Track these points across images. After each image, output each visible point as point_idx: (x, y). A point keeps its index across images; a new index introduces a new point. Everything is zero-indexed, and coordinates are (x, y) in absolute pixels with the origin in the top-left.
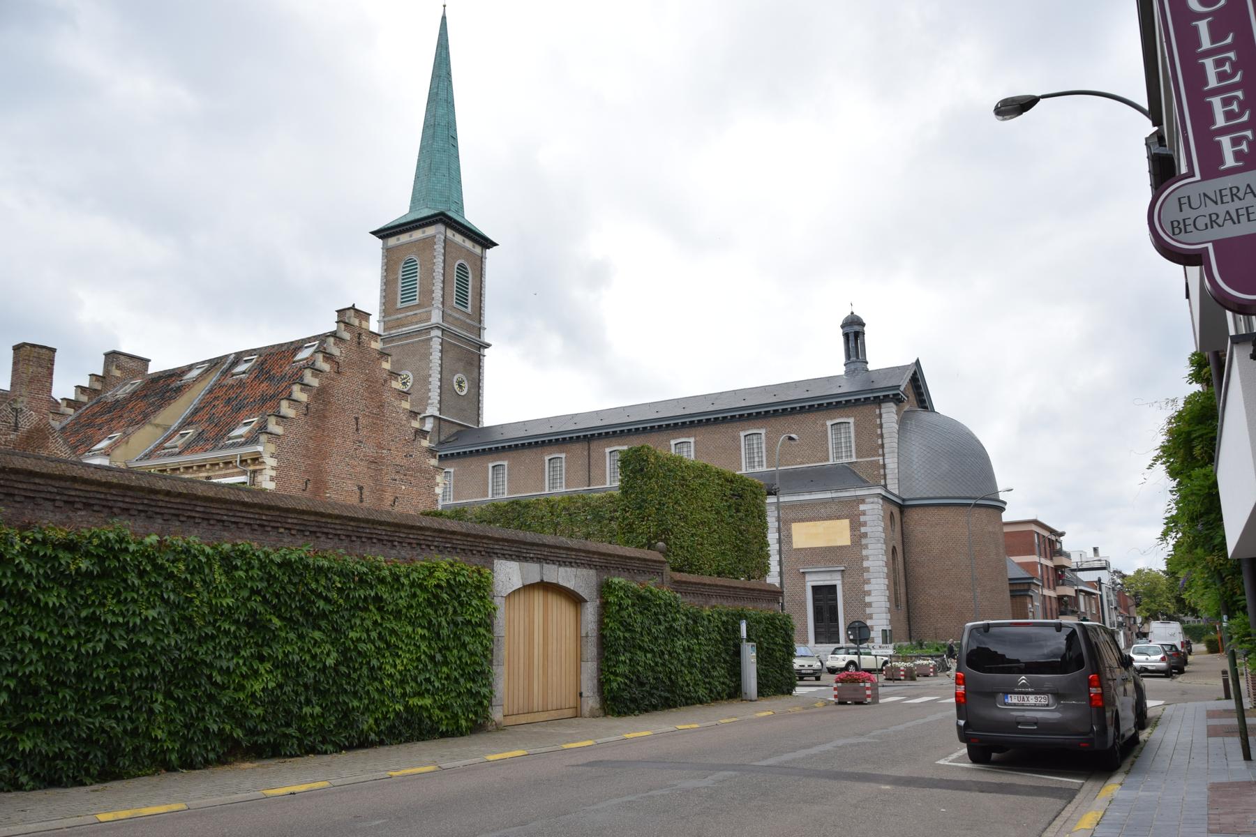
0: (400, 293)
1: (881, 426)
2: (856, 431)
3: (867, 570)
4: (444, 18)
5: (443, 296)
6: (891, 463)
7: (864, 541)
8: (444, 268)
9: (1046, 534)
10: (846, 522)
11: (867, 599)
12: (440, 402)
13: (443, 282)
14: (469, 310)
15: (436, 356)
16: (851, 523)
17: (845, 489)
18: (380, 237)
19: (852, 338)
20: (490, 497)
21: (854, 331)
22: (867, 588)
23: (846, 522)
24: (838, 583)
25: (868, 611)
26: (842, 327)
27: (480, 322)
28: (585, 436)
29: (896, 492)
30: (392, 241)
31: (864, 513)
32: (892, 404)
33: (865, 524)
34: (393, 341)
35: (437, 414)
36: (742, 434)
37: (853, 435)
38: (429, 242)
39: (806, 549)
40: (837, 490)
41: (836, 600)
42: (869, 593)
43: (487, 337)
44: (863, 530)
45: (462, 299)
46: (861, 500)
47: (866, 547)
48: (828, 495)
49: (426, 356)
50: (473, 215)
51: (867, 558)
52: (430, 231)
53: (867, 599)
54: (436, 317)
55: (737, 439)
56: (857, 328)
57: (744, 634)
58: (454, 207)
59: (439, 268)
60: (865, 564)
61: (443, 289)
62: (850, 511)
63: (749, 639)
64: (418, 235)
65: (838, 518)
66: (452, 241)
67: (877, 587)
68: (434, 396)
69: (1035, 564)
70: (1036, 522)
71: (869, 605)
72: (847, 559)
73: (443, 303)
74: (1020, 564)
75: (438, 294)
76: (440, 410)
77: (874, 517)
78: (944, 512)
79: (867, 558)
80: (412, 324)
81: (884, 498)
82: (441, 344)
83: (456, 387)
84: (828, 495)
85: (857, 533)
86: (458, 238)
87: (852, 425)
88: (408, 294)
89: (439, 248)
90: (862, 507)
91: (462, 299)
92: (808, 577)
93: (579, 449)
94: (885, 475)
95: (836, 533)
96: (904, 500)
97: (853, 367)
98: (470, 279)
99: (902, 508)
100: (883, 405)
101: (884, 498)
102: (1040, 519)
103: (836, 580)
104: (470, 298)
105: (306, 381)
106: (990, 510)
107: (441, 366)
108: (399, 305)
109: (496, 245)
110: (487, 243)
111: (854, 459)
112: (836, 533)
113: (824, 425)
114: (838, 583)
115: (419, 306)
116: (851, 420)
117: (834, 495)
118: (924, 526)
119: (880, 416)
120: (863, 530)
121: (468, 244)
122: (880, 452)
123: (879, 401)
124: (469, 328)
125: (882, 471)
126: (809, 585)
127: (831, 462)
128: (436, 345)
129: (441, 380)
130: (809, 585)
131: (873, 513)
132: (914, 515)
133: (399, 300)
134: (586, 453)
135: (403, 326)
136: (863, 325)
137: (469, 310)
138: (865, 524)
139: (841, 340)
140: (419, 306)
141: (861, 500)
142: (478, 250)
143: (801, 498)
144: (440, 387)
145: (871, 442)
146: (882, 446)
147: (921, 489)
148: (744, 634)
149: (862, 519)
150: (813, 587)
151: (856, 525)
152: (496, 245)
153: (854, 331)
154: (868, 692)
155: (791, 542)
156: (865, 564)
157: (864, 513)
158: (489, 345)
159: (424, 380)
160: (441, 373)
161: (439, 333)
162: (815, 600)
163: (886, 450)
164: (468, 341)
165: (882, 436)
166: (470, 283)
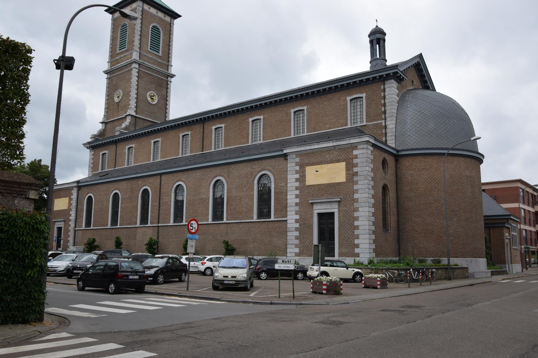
0: (118, 44)
1: (384, 98)
2: (367, 103)
3: (357, 200)
5: (140, 44)
6: (391, 124)
7: (355, 179)
8: (141, 27)
9: (531, 191)
10: (343, 164)
11: (356, 223)
12: (136, 107)
13: (141, 35)
14: (160, 54)
15: (134, 80)
16: (347, 165)
17: (342, 139)
18: (111, 13)
19: (375, 42)
20: (151, 161)
21: (377, 38)
22: (356, 214)
23: (343, 164)
24: (336, 211)
25: (356, 232)
27: (168, 61)
28: (201, 119)
29: (393, 146)
31: (356, 157)
32: (393, 81)
33: (356, 165)
34: (114, 73)
35: (134, 114)
36: (292, 111)
37: (364, 106)
39: (314, 185)
40: (337, 140)
41: (333, 223)
42: (357, 219)
43: (173, 70)
44: (355, 170)
45: (155, 46)
46: (354, 147)
47: (357, 183)
48: (331, 144)
49: (129, 80)
51: (357, 191)
53: (356, 223)
54: (135, 56)
55: (289, 114)
56: (379, 36)
60: (356, 196)
61: (140, 40)
62: (346, 156)
65: (338, 161)
66: (148, 12)
68: (133, 103)
69: (519, 209)
70: (520, 181)
71: (357, 228)
72: (341, 192)
73: (140, 48)
74: (507, 209)
76: (136, 112)
77: (363, 160)
78: (429, 160)
79: (357, 191)
81: (374, 145)
82: (138, 73)
83: (149, 99)
84: (331, 144)
85: (351, 172)
86: (153, 11)
87: (364, 98)
88: (122, 46)
90: (355, 152)
91: (155, 46)
92: (315, 207)
93: (198, 128)
94: (386, 134)
95: (333, 173)
96: (398, 151)
97: (375, 63)
99: (397, 157)
100: (386, 82)
101: (374, 145)
103: (334, 209)
104: (161, 47)
106: (468, 160)
107: (137, 85)
108: (118, 52)
109: (180, 16)
110: (175, 16)
111: (365, 124)
112: (333, 173)
114: (336, 211)
115: (127, 51)
116: (364, 95)
117: (335, 144)
118: (412, 170)
119: (384, 90)
120: (355, 170)
121: (160, 15)
122: (383, 116)
124: (159, 64)
125: (384, 131)
126: (316, 212)
127: (349, 126)
128: (135, 73)
129: (137, 94)
130: (316, 212)
131: (364, 156)
132: (406, 163)
133: (118, 49)
134: (202, 130)
136: (385, 34)
137: (160, 54)
138: (356, 165)
139: (368, 45)
140: (127, 51)
141: (354, 147)
142: (168, 19)
143: (312, 147)
144: (137, 98)
145: (377, 111)
146: (385, 112)
147: (413, 141)
149: (355, 161)
150: (320, 215)
151: (350, 166)
152: (180, 16)
153: (377, 38)
155: (305, 181)
156: (356, 196)
157: (356, 157)
158: (173, 76)
159: (127, 94)
160: (137, 89)
161: (137, 66)
162: (320, 224)
163: (387, 115)
164: (159, 72)
165: (384, 105)
166: (161, 38)
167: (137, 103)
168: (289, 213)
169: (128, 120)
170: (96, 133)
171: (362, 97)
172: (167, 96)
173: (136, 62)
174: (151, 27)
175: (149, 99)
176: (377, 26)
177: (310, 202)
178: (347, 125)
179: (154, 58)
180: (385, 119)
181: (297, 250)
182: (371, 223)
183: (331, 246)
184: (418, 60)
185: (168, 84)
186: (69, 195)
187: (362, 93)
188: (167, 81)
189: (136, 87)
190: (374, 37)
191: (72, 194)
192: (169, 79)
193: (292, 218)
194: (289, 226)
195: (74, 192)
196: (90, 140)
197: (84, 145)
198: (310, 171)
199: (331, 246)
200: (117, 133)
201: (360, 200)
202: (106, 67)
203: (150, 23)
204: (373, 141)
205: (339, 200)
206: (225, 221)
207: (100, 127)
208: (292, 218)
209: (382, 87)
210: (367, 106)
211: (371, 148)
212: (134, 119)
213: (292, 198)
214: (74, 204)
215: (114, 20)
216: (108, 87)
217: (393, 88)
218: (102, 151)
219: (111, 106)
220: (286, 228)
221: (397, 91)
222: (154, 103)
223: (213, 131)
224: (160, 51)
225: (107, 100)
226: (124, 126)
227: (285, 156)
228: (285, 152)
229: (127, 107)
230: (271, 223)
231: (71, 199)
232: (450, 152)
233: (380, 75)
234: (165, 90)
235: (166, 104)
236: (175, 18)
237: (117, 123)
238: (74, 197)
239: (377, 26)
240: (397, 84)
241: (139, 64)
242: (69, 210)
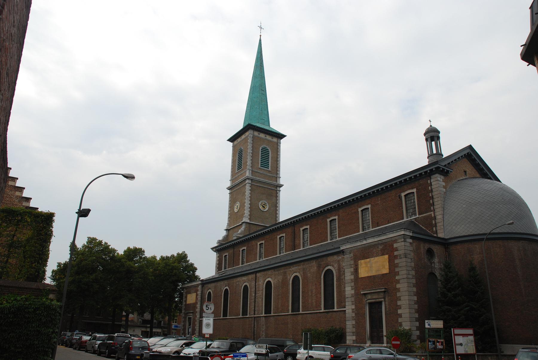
4: (260, 40)
12: (250, 215)
26: (425, 135)
30: (236, 142)
32: (437, 175)
35: (248, 221)
41: (382, 312)
43: (282, 181)
45: (265, 163)
46: (395, 240)
50: (275, 125)
56: (432, 134)
66: (258, 137)
68: (247, 212)
72: (386, 283)
76: (250, 219)
83: (261, 207)
86: (262, 135)
91: (265, 163)
93: (290, 230)
101: (412, 237)
112: (375, 266)
113: (400, 197)
121: (269, 138)
128: (248, 187)
133: (237, 169)
136: (439, 132)
137: (270, 169)
142: (275, 140)
146: (433, 204)
150: (370, 304)
158: (281, 186)
159: (242, 206)
160: (250, 201)
161: (250, 182)
167: (250, 212)
168: (347, 304)
169: (243, 227)
170: (221, 238)
171: (413, 193)
172: (277, 203)
173: (249, 179)
174: (261, 149)
175: (261, 207)
176: (431, 126)
177: (362, 293)
179: (264, 173)
181: (354, 338)
182: (414, 311)
183: (381, 334)
184: (468, 151)
185: (277, 193)
186: (196, 291)
187: (412, 188)
188: (277, 191)
189: (249, 199)
190: (429, 135)
191: (198, 290)
192: (278, 189)
193: (349, 308)
194: (347, 315)
195: (200, 288)
196: (216, 245)
197: (212, 249)
198: (362, 263)
199: (381, 334)
200: (235, 238)
201: (401, 290)
202: (229, 184)
204: (411, 234)
205: (383, 290)
206: (301, 312)
207: (224, 233)
208: (349, 308)
209: (429, 181)
210: (418, 201)
211: (411, 241)
212: (248, 225)
213: (349, 291)
214: (199, 299)
215: (234, 147)
216: (230, 201)
217: (439, 182)
218: (224, 253)
219: (233, 216)
220: (345, 317)
221: (444, 184)
222: (265, 210)
223: (301, 232)
224: (270, 167)
225: (229, 211)
226: (239, 232)
227: (343, 252)
228: (342, 248)
229: (242, 216)
230: (335, 313)
231: (197, 295)
232: (489, 237)
233: (439, 167)
234: (275, 198)
235: (276, 210)
236: (282, 138)
237: (236, 229)
238: (199, 293)
239: (431, 126)
240: (442, 177)
241: (252, 180)
242: (196, 303)
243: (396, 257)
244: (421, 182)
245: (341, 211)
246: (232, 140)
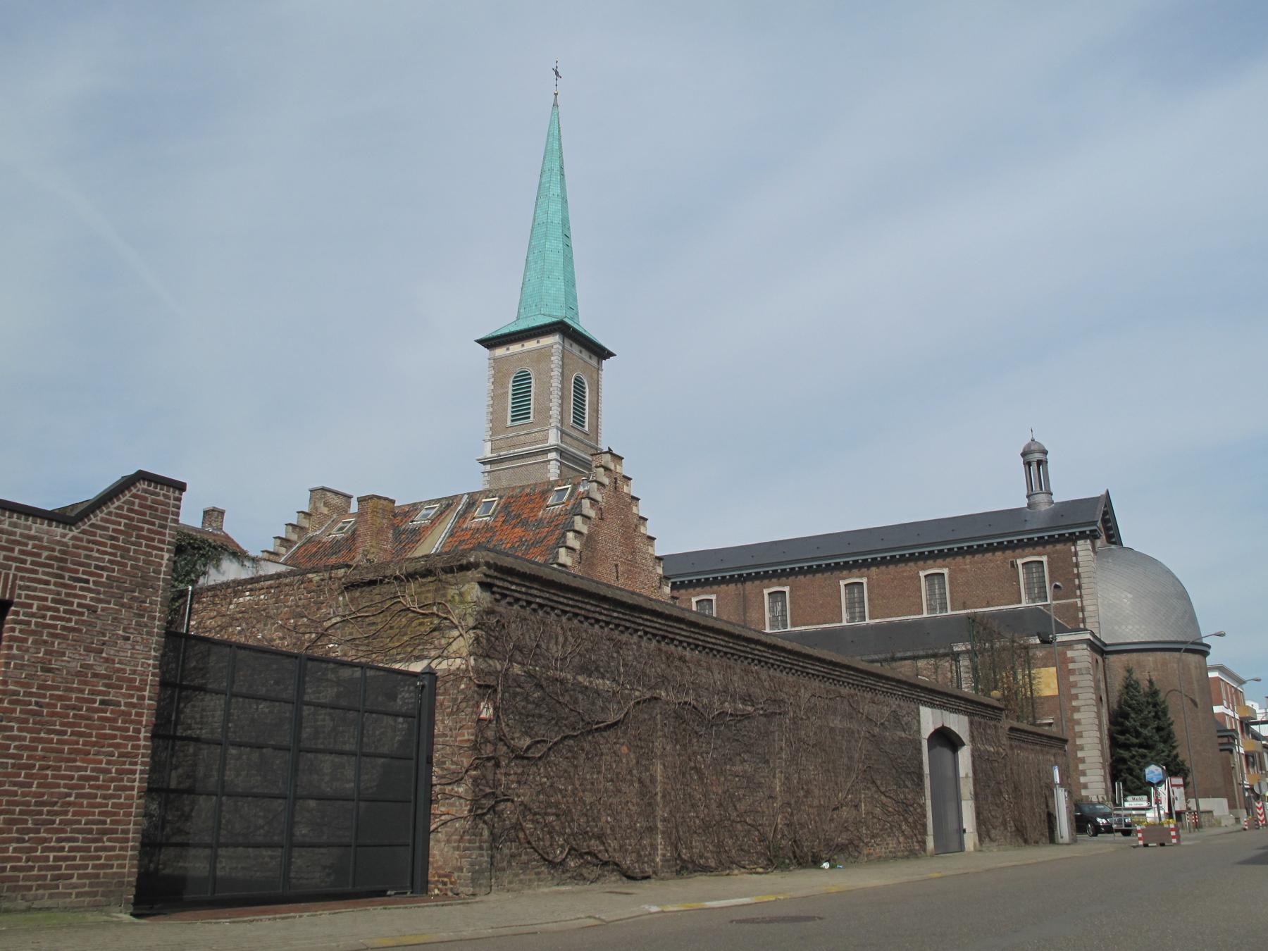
0: (510, 410)
19: (1034, 467)
21: (1035, 460)
30: (500, 352)
38: (543, 354)
52: (546, 341)
54: (553, 438)
57: (1057, 779)
58: (571, 313)
59: (556, 383)
63: (1061, 785)
64: (531, 345)
67: (1090, 740)
75: (555, 411)
80: (524, 444)
82: (560, 468)
89: (556, 359)
96: (1106, 645)
98: (587, 394)
102: (1227, 665)
105: (577, 528)
109: (613, 355)
110: (601, 353)
113: (1013, 565)
123: (1073, 539)
127: (1024, 604)
133: (509, 418)
135: (515, 446)
136: (1045, 453)
137: (587, 428)
142: (594, 362)
145: (1068, 582)
146: (1080, 587)
148: (1057, 779)
152: (613, 355)
154: (1173, 833)
165: (1078, 576)
166: (587, 399)
178: (1020, 602)
180: (1081, 597)
203: (573, 372)
224: (586, 424)
243: (1072, 672)
244: (1059, 547)
245: (874, 569)
246: (490, 343)
